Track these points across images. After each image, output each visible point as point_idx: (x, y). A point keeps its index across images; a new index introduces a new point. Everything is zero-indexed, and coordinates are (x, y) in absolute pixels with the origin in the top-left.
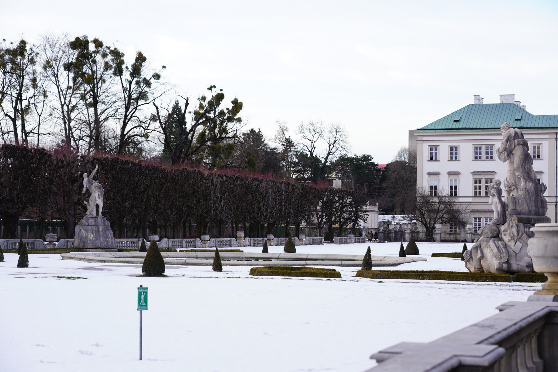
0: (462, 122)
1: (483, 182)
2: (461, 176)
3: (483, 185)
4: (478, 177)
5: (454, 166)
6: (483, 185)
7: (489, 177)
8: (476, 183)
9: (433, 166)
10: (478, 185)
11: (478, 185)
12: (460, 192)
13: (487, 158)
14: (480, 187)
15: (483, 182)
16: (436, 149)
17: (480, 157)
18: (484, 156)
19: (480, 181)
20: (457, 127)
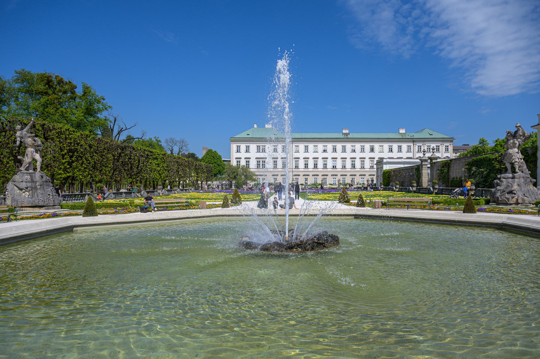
0: (250, 135)
1: (261, 162)
2: (337, 159)
3: (261, 163)
4: (259, 160)
5: (248, 155)
6: (261, 163)
7: (264, 160)
8: (258, 162)
9: (238, 155)
10: (264, 163)
11: (264, 163)
12: (251, 166)
13: (263, 151)
14: (260, 164)
15: (261, 162)
16: (239, 147)
17: (260, 151)
18: (261, 151)
19: (260, 162)
20: (249, 137)
